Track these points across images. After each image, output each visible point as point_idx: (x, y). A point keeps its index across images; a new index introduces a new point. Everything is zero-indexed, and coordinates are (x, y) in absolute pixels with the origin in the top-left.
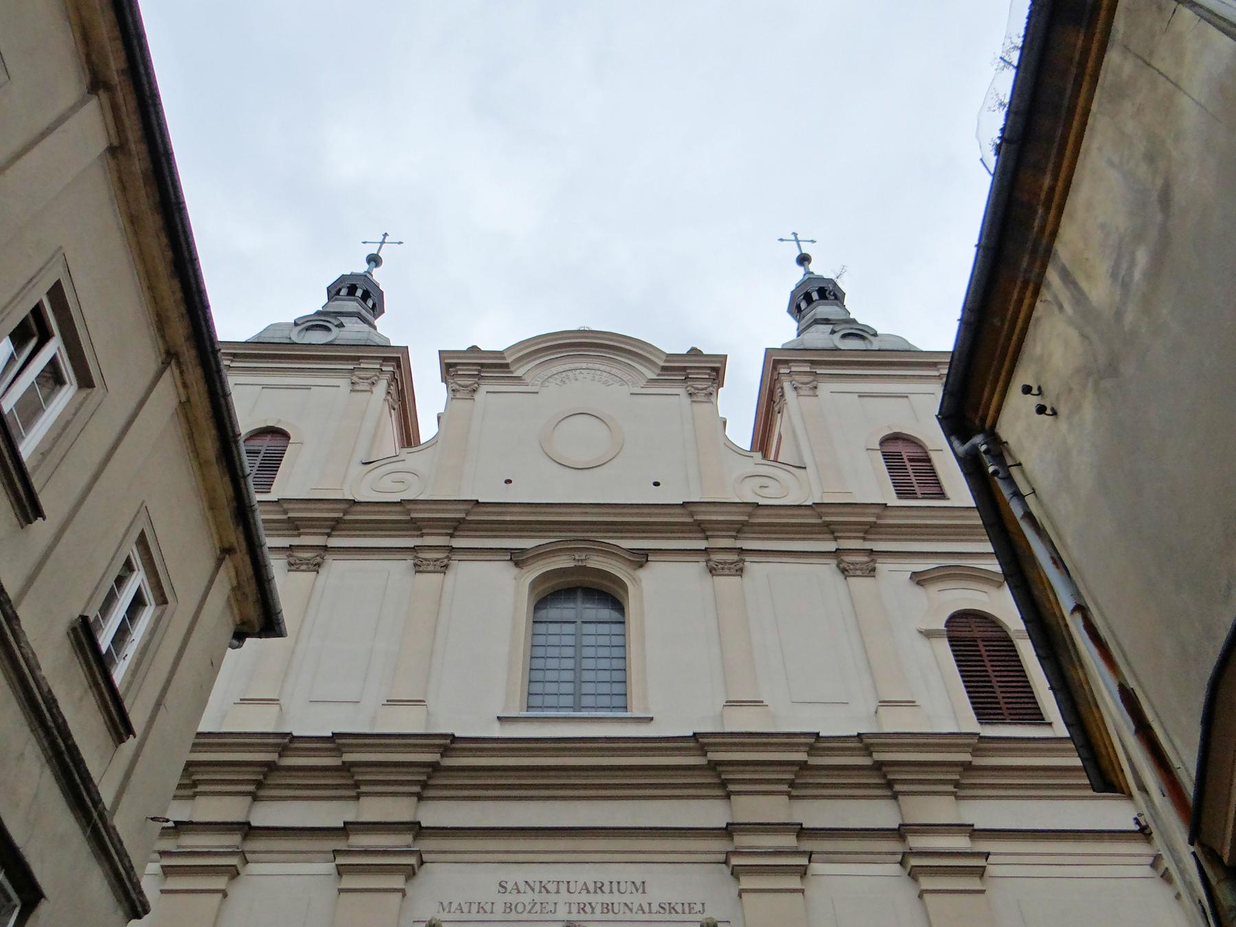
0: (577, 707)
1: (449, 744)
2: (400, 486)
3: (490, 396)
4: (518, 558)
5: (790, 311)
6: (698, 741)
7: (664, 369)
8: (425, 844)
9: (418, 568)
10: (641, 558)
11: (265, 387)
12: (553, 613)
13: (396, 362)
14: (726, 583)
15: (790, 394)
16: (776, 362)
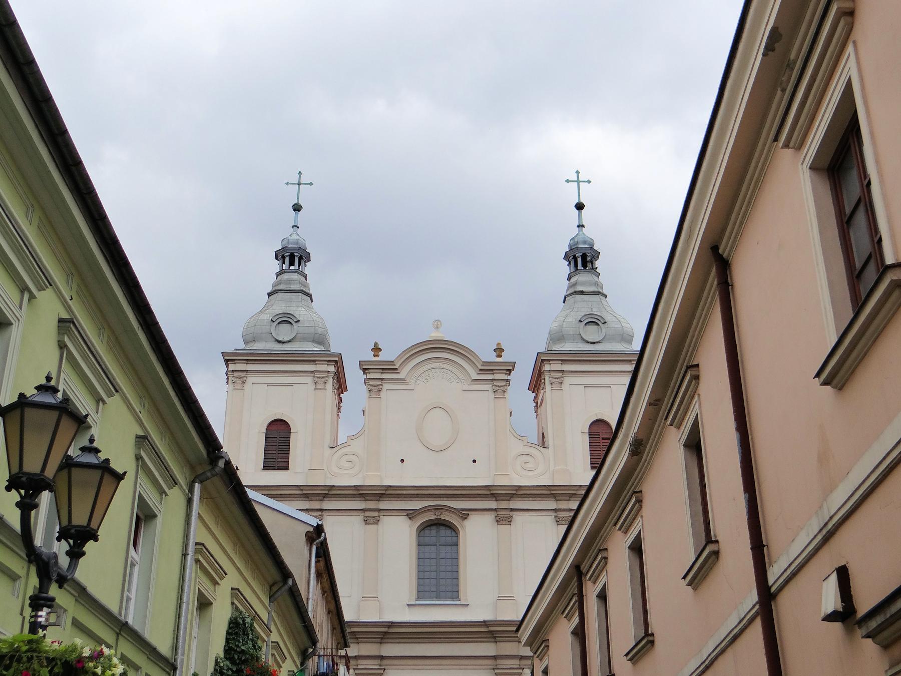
0: (438, 597)
1: (391, 624)
2: (349, 465)
3: (391, 395)
4: (411, 515)
5: (566, 257)
6: (485, 623)
7: (481, 370)
8: (385, 662)
9: (367, 521)
10: (464, 515)
11: (269, 385)
12: (427, 532)
13: (338, 363)
14: (504, 528)
15: (548, 386)
16: (541, 361)
